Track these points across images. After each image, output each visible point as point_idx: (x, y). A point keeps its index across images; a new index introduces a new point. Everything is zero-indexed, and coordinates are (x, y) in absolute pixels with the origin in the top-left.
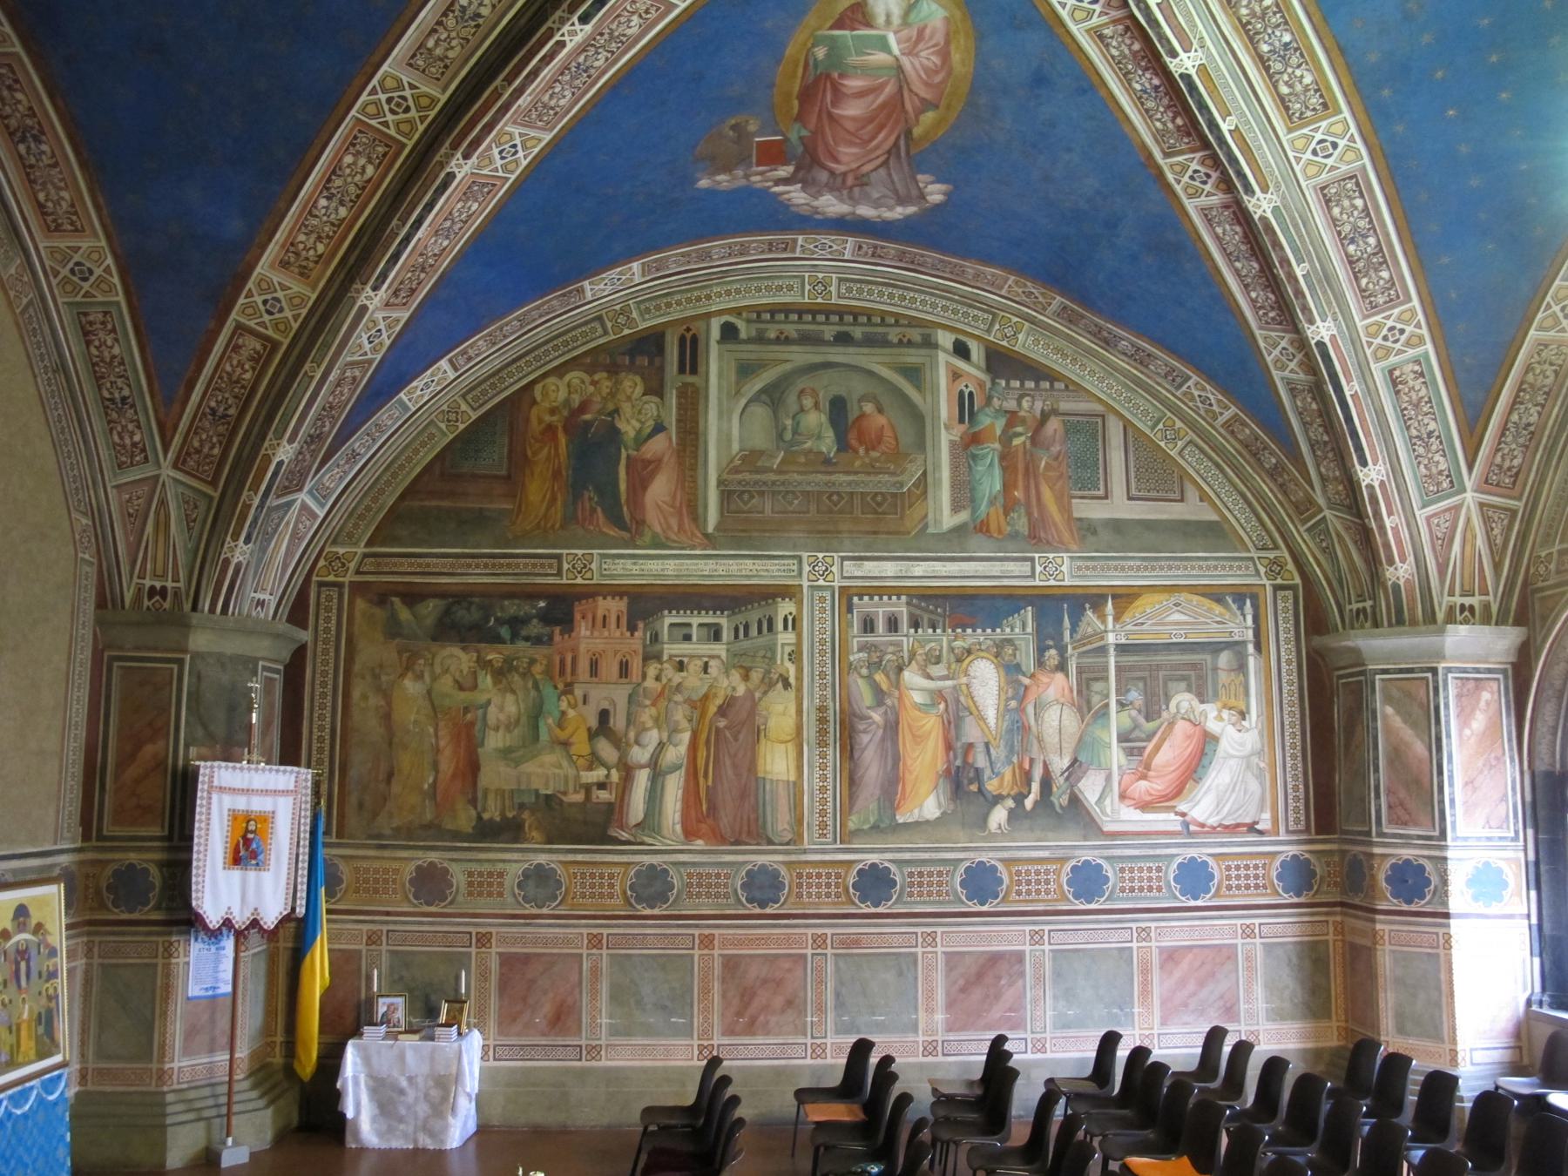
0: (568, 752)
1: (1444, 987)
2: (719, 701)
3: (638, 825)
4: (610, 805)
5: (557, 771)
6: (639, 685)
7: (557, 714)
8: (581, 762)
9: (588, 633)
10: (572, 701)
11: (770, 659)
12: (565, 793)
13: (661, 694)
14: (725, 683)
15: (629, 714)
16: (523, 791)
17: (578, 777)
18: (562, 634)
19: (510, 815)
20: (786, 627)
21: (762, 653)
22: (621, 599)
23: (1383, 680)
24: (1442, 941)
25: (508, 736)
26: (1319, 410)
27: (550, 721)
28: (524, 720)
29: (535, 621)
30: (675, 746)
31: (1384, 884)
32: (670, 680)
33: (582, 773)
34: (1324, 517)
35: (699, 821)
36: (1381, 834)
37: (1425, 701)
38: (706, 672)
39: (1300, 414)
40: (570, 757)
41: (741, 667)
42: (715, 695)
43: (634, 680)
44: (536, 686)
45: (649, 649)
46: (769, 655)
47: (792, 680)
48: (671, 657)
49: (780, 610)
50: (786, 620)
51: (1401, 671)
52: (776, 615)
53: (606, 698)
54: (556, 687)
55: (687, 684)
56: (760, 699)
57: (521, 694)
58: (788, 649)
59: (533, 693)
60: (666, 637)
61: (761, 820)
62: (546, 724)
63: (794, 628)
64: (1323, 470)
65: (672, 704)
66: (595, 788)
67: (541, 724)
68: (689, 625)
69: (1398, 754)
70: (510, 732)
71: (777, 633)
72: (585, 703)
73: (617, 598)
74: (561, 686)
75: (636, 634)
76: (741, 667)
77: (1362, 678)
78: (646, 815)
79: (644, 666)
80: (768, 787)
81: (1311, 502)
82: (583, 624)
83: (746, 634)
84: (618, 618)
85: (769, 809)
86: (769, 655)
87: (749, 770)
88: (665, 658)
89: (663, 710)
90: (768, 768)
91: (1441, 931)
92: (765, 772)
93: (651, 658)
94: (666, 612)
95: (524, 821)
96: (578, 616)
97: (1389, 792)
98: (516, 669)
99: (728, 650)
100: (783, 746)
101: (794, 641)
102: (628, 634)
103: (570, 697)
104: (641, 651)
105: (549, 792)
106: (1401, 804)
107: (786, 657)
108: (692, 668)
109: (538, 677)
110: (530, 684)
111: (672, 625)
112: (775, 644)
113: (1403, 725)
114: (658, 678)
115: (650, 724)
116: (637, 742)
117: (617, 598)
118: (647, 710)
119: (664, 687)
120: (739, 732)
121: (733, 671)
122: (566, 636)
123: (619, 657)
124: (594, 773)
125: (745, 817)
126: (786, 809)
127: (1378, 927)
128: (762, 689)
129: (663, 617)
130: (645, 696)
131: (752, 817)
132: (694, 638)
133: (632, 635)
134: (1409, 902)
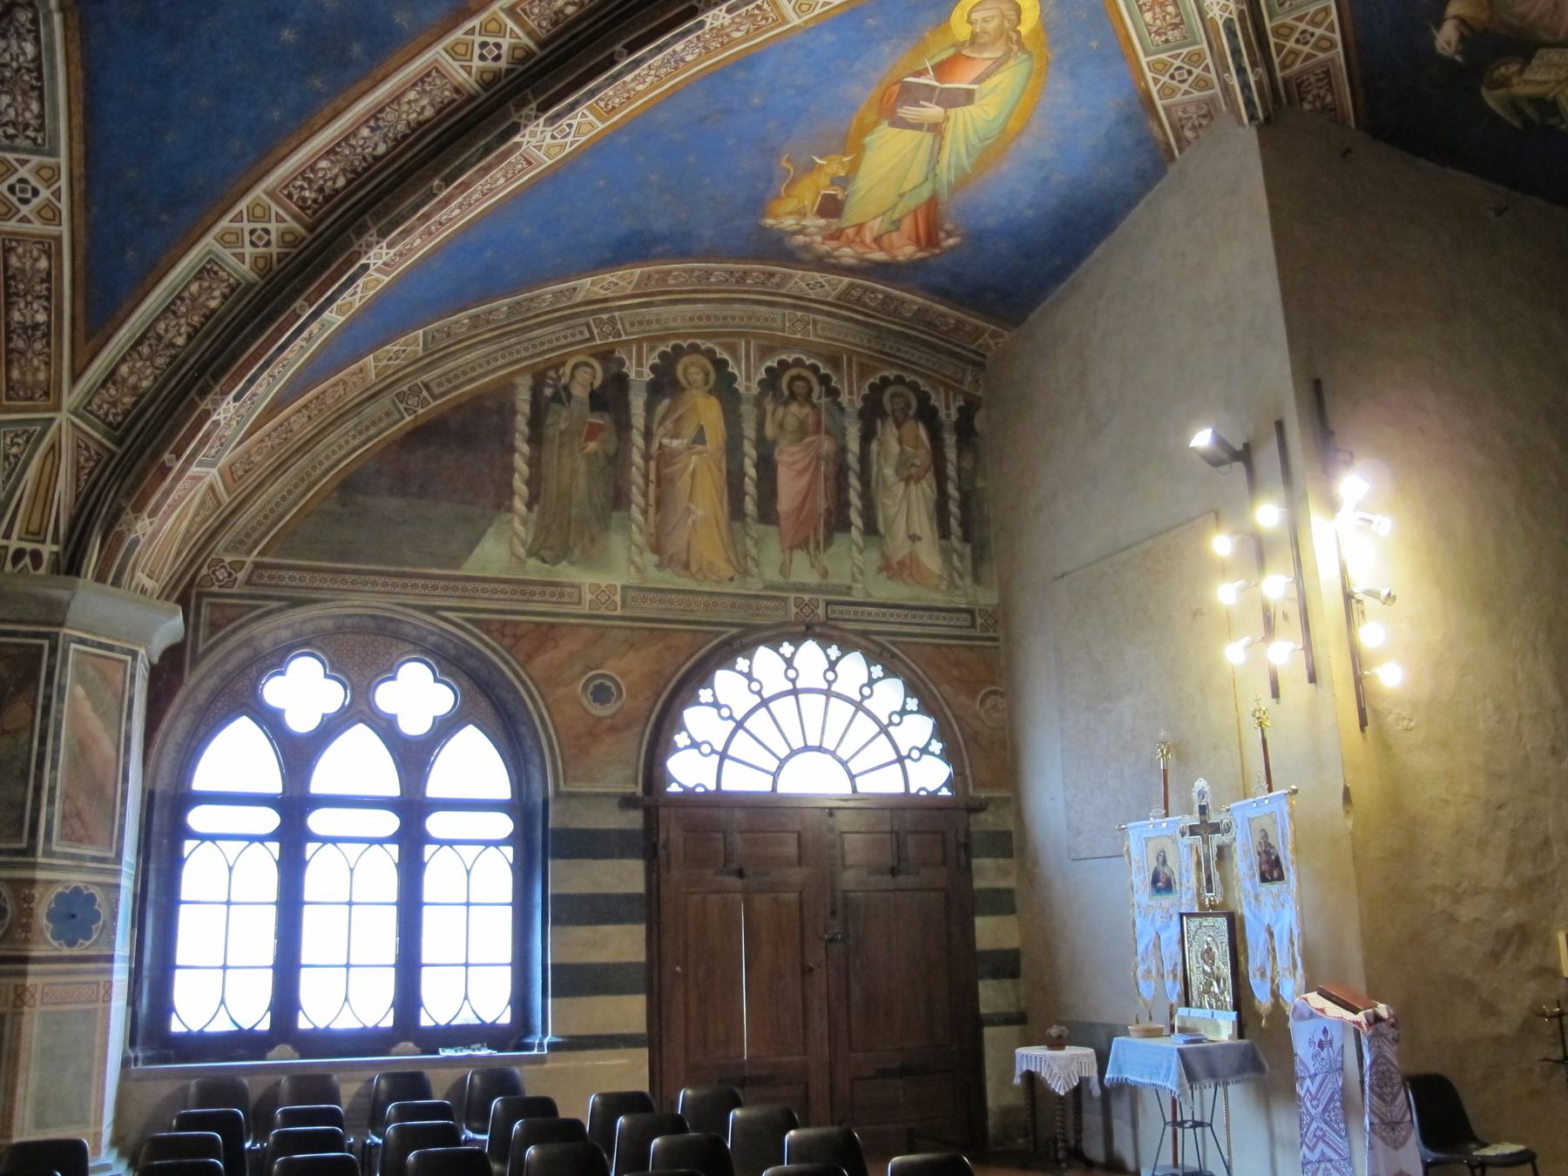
1: (97, 1052)
23: (78, 651)
24: (102, 992)
26: (213, 311)
31: (45, 921)
34: (52, 420)
36: (48, 853)
37: (121, 689)
39: (180, 297)
51: (100, 645)
64: (124, 369)
69: (82, 749)
77: (46, 643)
81: (50, 392)
91: (102, 978)
97: (67, 796)
106: (78, 815)
113: (92, 714)
127: (30, 981)
134: (71, 943)
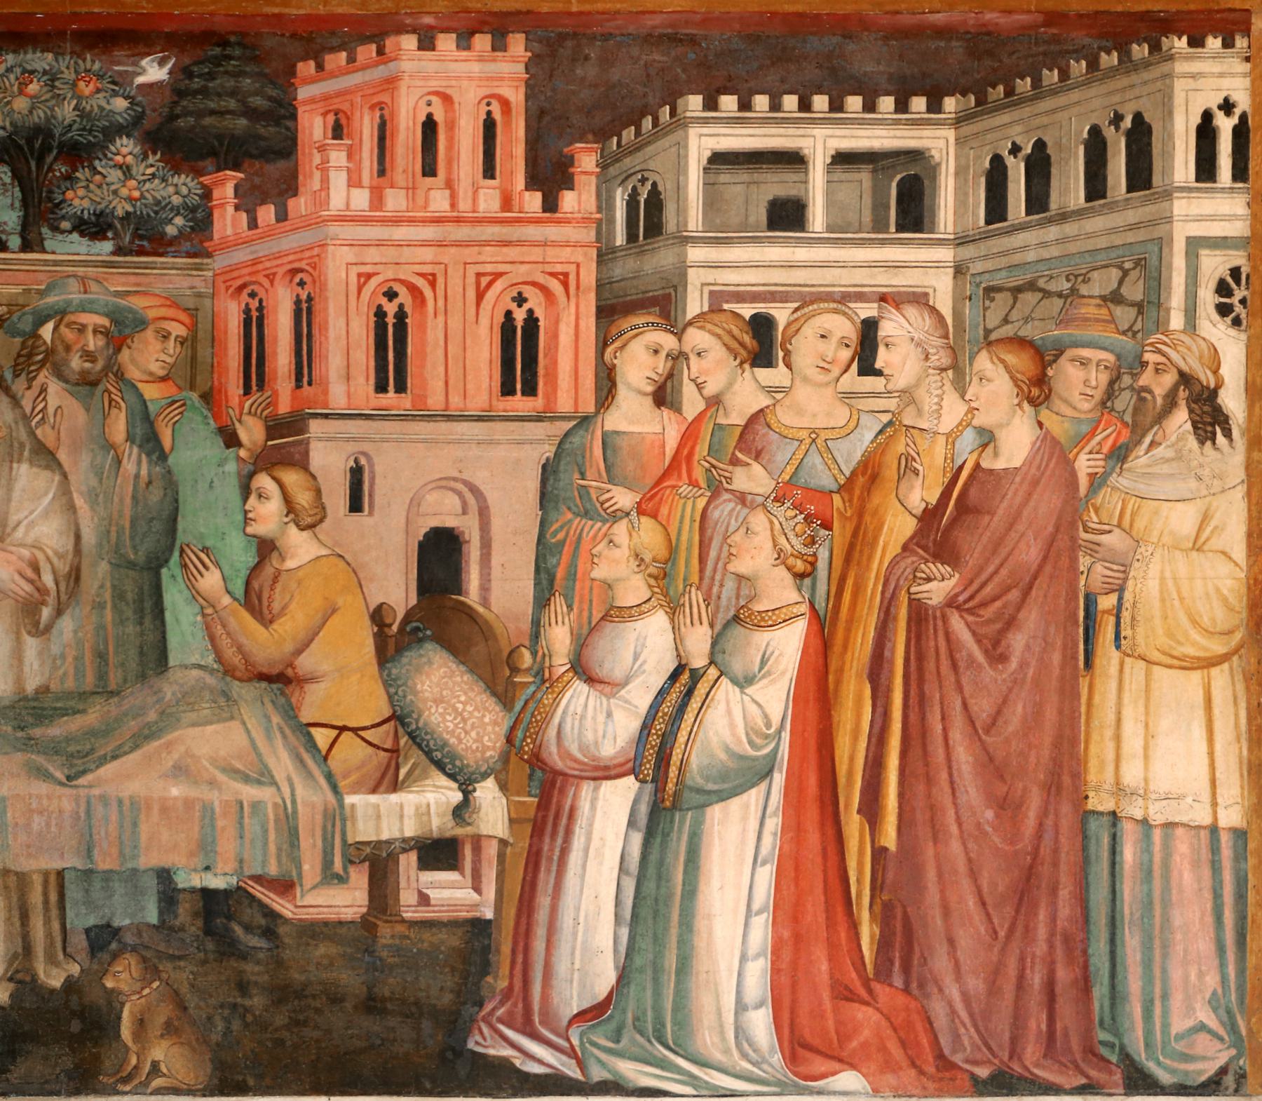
0: (290, 713)
2: (922, 494)
3: (594, 1013)
4: (479, 927)
5: (250, 792)
6: (585, 421)
7: (241, 556)
8: (350, 753)
9: (361, 199)
10: (303, 498)
11: (1140, 307)
12: (285, 886)
13: (681, 460)
14: (953, 411)
15: (544, 549)
16: (108, 876)
17: (336, 818)
18: (248, 200)
19: (54, 979)
20: (1206, 168)
21: (1104, 282)
22: (499, 45)
25: (31, 645)
27: (211, 581)
28: (98, 575)
29: (126, 147)
30: (744, 682)
32: (715, 402)
33: (349, 799)
35: (844, 994)
38: (867, 367)
40: (304, 730)
41: (1021, 343)
42: (908, 467)
43: (564, 403)
44: (151, 443)
45: (619, 270)
46: (1134, 291)
47: (1233, 401)
48: (718, 299)
49: (1180, 86)
50: (1206, 132)
52: (1169, 114)
53: (444, 484)
54: (231, 440)
55: (785, 417)
56: (1097, 482)
57: (80, 467)
58: (1214, 265)
59: (134, 463)
60: (695, 220)
61: (1100, 991)
62: (195, 594)
63: (1240, 173)
65: (724, 510)
66: (408, 862)
67: (174, 595)
68: (794, 160)
70: (40, 631)
71: (1167, 195)
72: (356, 505)
73: (482, 42)
74: (251, 432)
75: (568, 200)
76: (1021, 343)
78: (623, 978)
79: (603, 343)
80: (1128, 854)
82: (338, 157)
83: (1037, 201)
84: (489, 127)
85: (1131, 943)
86: (1134, 291)
87: (1053, 787)
88: (694, 305)
89: (689, 536)
90: (1132, 774)
92: (1119, 789)
93: (630, 308)
94: (695, 102)
95: (113, 1000)
96: (313, 126)
98: (53, 360)
99: (959, 270)
100: (1196, 677)
101: (1239, 229)
102: (534, 201)
103: (292, 478)
104: (589, 276)
105: (216, 882)
107: (1207, 297)
108: (806, 348)
109: (151, 392)
110: (119, 427)
111: (719, 159)
112: (1162, 243)
114: (664, 396)
115: (634, 590)
116: (581, 669)
117: (482, 42)
118: (621, 529)
119: (690, 435)
120: (1010, 623)
121: (984, 362)
122: (267, 214)
123: (498, 299)
124: (408, 799)
125: (1036, 979)
126: (1205, 945)
128: (1106, 436)
129: (680, 122)
130: (612, 477)
131: (1063, 975)
132: (817, 218)
133: (550, 205)
